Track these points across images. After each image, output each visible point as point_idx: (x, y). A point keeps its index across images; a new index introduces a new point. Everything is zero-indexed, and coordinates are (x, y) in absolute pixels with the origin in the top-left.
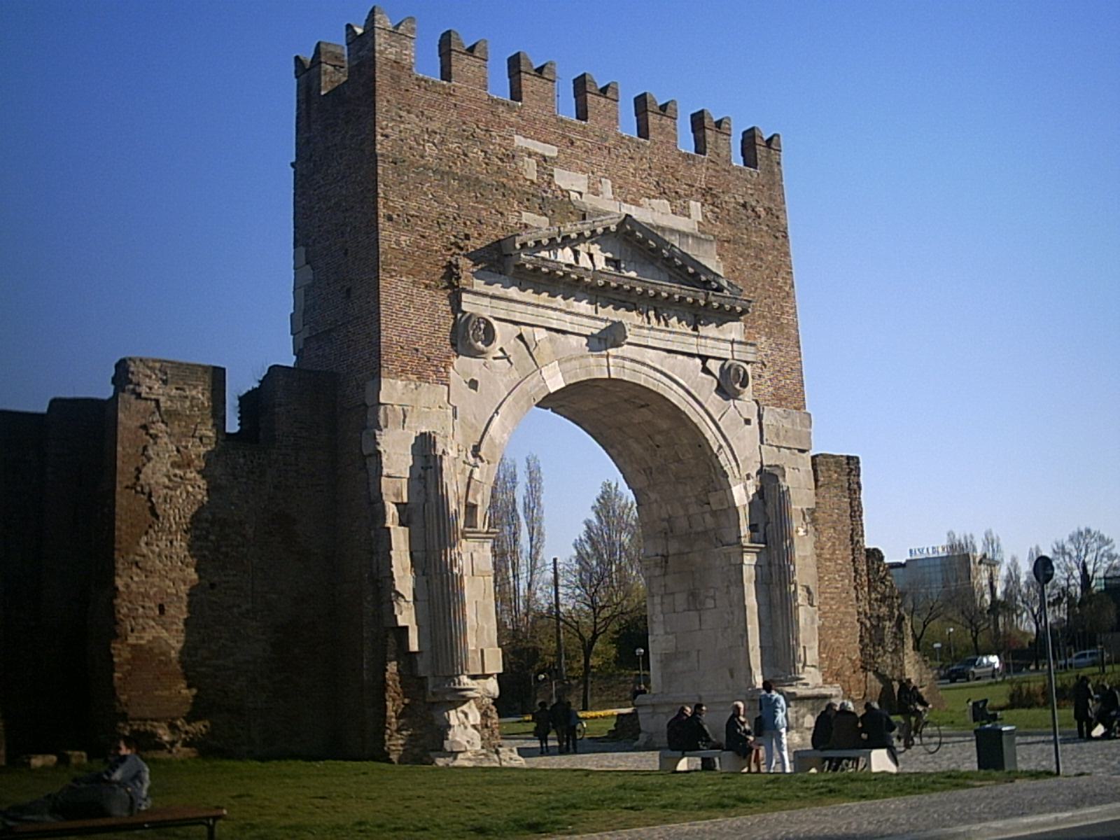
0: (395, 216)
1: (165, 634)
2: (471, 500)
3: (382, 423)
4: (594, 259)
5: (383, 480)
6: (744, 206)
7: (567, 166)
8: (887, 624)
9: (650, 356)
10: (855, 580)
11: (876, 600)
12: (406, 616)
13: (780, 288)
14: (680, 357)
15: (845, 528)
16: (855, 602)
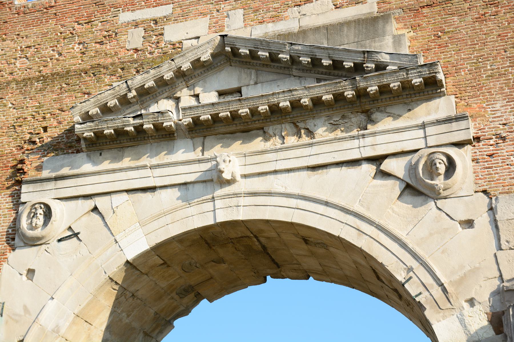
14: (334, 171)
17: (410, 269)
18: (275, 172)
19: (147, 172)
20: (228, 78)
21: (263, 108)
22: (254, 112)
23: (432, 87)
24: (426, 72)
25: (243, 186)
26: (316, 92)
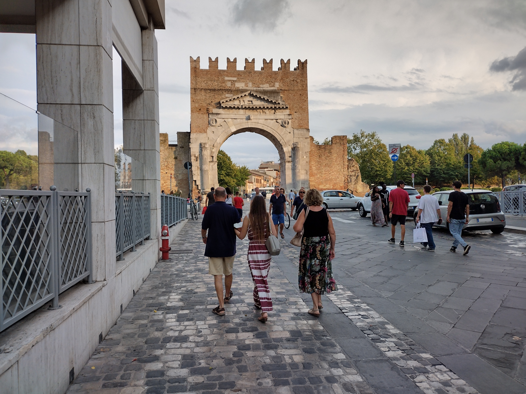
4: (246, 101)
7: (239, 81)
12: (197, 177)
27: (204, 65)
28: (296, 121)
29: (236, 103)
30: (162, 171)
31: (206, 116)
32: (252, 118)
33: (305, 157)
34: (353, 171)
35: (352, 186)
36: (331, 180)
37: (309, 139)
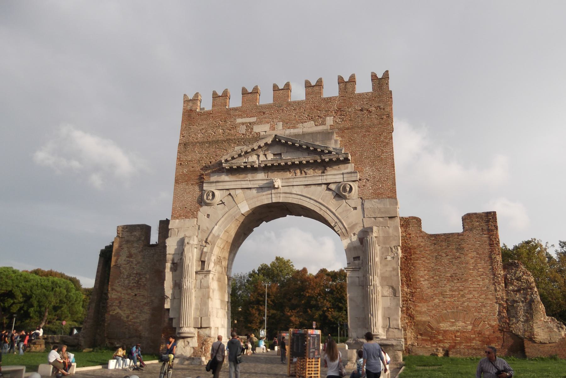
0: (182, 163)
1: (120, 312)
2: (203, 259)
3: (169, 235)
5: (168, 256)
6: (361, 110)
8: (521, 304)
9: (295, 190)
10: (494, 280)
11: (514, 291)
13: (383, 141)
14: (313, 187)
15: (485, 252)
16: (493, 292)
17: (336, 223)
18: (293, 186)
19: (249, 182)
20: (277, 150)
21: (289, 163)
22: (286, 164)
23: (346, 161)
24: (345, 156)
25: (282, 190)
26: (308, 159)
27: (206, 104)
28: (369, 184)
29: (253, 158)
30: (130, 291)
31: (197, 188)
32: (278, 183)
33: (389, 258)
34: (518, 291)
35: (520, 325)
36: (467, 310)
37: (398, 220)
